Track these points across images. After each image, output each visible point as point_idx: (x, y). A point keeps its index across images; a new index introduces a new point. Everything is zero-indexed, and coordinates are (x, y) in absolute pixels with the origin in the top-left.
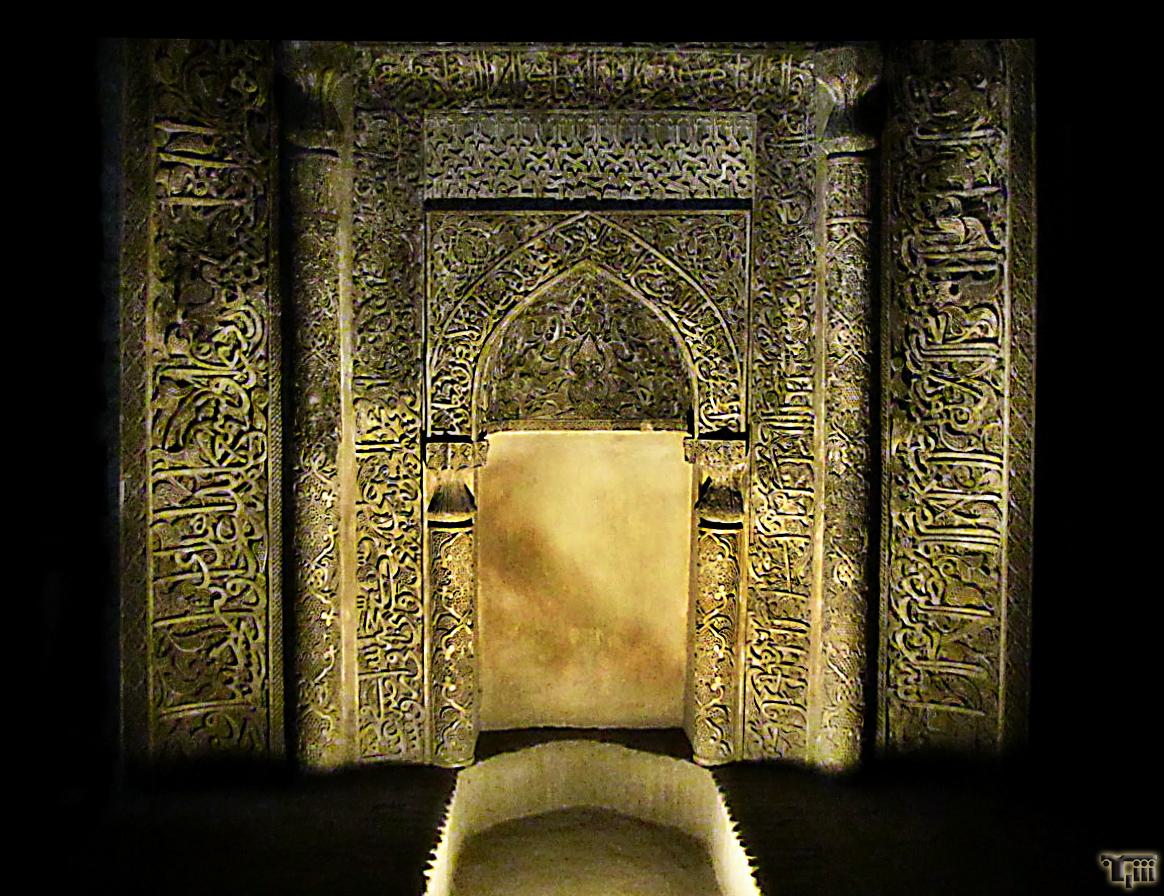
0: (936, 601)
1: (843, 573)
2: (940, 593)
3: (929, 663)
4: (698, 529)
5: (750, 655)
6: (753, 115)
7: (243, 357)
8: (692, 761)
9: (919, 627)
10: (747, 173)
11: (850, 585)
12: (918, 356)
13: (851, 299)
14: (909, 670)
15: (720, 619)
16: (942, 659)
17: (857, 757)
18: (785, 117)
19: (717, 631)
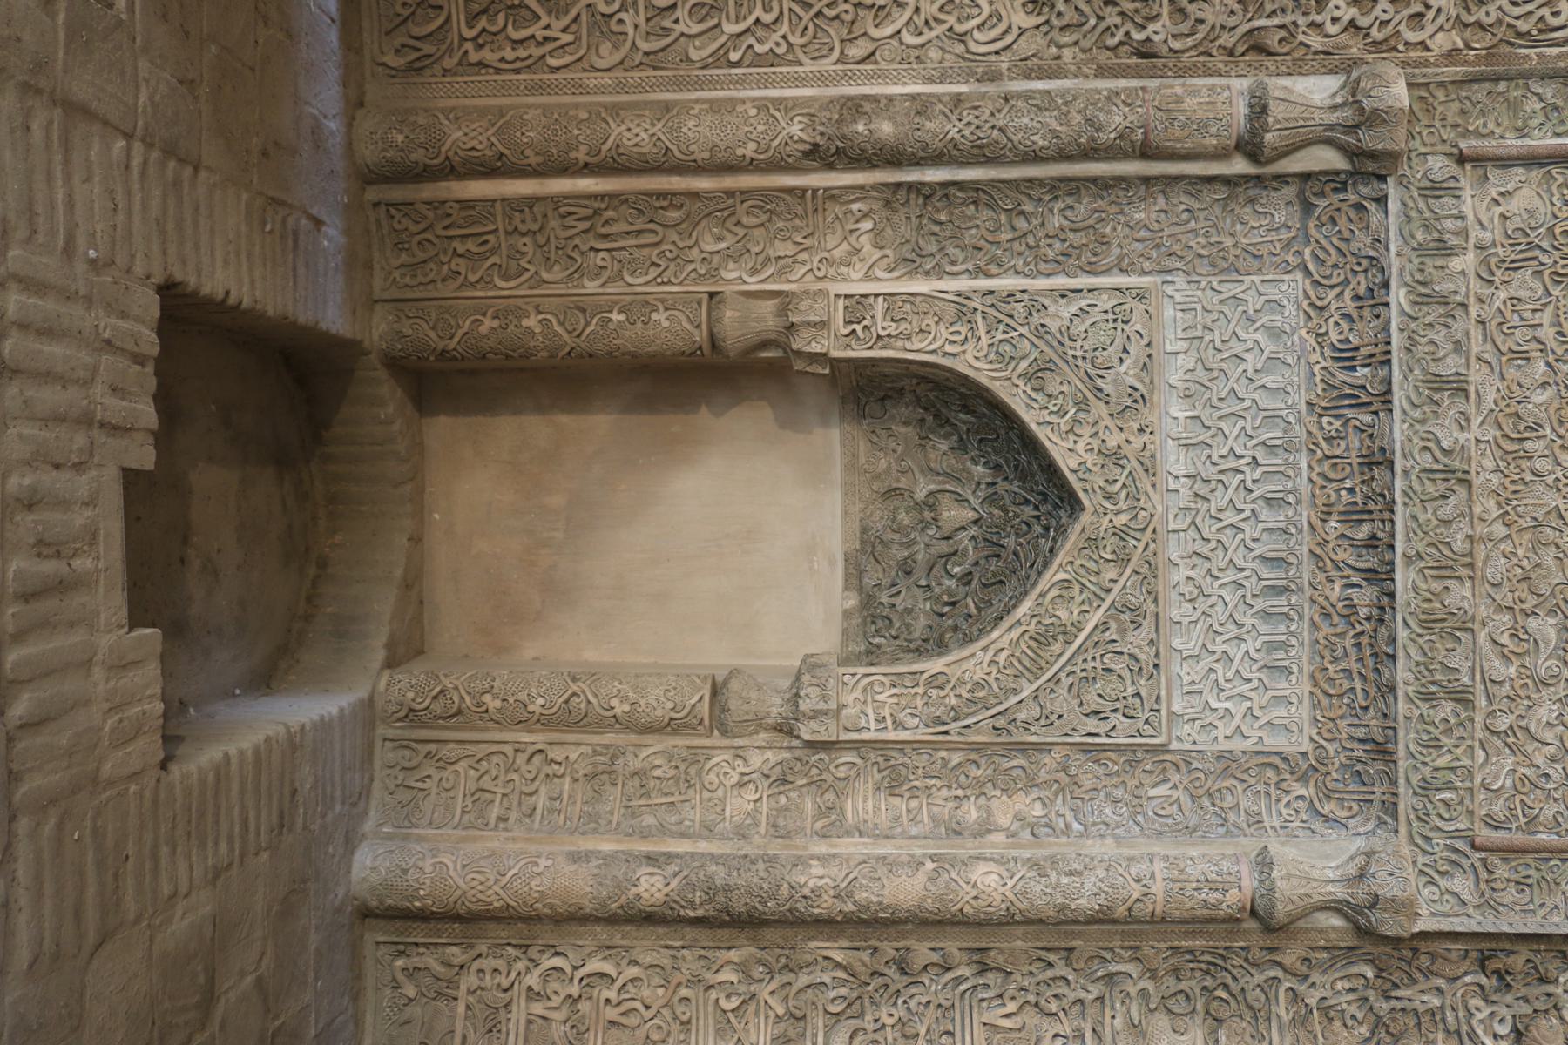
0: (611, 1013)
1: (653, 879)
2: (623, 1020)
3: (523, 1004)
4: (709, 672)
5: (531, 749)
6: (1306, 746)
7: (946, 26)
8: (382, 668)
9: (575, 990)
10: (1221, 739)
11: (634, 890)
12: (962, 988)
13: (1042, 893)
14: (513, 975)
15: (583, 706)
16: (529, 1022)
17: (390, 901)
18: (1303, 792)
19: (566, 702)
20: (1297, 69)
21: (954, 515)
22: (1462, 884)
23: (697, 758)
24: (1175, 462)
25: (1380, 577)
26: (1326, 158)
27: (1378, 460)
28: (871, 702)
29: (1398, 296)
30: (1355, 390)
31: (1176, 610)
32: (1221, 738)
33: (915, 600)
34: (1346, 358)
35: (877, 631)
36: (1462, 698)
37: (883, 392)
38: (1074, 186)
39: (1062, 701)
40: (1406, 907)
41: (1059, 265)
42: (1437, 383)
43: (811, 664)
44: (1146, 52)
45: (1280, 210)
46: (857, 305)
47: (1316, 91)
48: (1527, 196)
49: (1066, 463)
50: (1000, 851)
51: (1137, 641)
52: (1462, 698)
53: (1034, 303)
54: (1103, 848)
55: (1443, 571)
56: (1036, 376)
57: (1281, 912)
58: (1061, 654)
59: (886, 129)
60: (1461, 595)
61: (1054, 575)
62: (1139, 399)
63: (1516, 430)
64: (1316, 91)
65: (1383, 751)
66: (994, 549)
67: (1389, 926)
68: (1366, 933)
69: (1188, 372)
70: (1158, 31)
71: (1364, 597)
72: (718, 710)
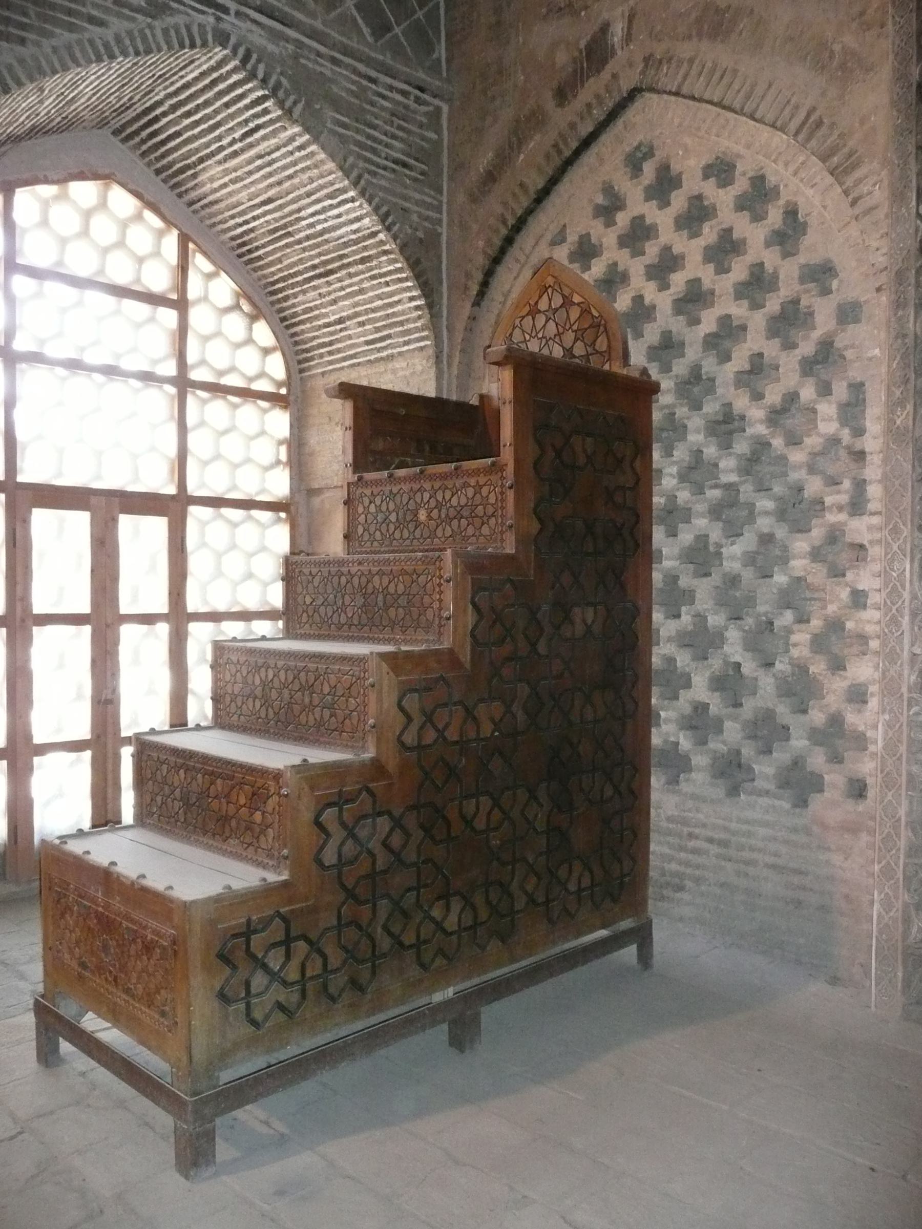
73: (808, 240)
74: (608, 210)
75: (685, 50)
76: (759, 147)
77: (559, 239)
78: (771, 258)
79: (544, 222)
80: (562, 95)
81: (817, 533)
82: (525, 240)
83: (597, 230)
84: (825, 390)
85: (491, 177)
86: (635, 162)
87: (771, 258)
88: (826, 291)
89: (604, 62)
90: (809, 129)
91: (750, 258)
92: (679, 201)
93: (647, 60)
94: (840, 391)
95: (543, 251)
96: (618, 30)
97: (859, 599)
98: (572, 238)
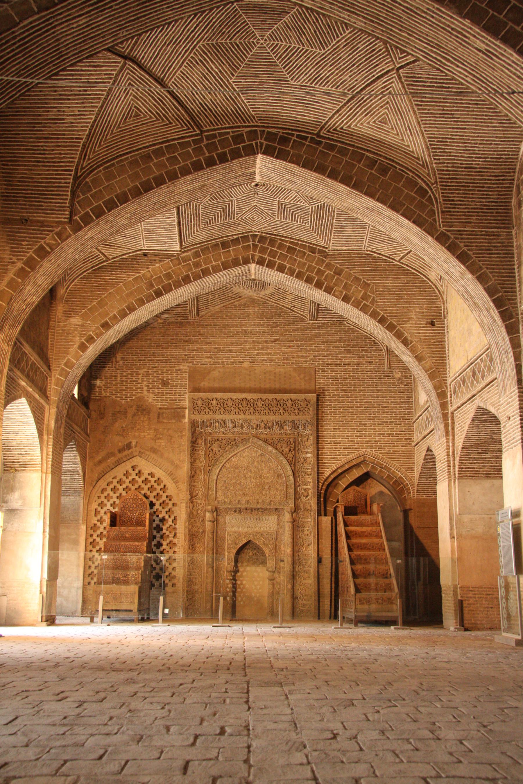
20: (205, 516)
21: (251, 554)
22: (290, 502)
23: (277, 582)
24: (246, 530)
25: (258, 509)
26: (215, 513)
27: (246, 509)
28: (271, 564)
29: (230, 506)
30: (240, 511)
31: (262, 529)
32: (275, 525)
33: (260, 559)
34: (235, 511)
35: (263, 563)
36: (271, 501)
37: (236, 561)
38: (216, 540)
39: (271, 542)
40: (291, 508)
41: (224, 542)
42: (238, 503)
43: (267, 570)
44: (203, 532)
45: (220, 518)
46: (228, 564)
47: (208, 515)
48: (220, 493)
49: (246, 541)
50: (286, 550)
51: (265, 534)
52: (271, 501)
53: (228, 544)
54: (286, 539)
55: (258, 503)
56: (236, 544)
57: (292, 520)
58: (266, 542)
59: (210, 560)
60: (260, 501)
61: (257, 543)
62: (239, 534)
63: (244, 495)
64: (208, 515)
65: (276, 509)
66: (255, 549)
67: (293, 510)
68: (295, 512)
69: (237, 528)
70: (201, 531)
71: (260, 510)
72: (272, 579)
73: (168, 491)
74: (127, 474)
75: (148, 453)
76: (159, 473)
77: (115, 478)
78: (161, 493)
79: (112, 474)
80: (120, 451)
81: (168, 541)
82: (107, 476)
83: (124, 478)
84: (169, 517)
85: (100, 462)
86: (133, 468)
87: (161, 493)
88: (170, 500)
89: (130, 449)
90: (171, 474)
91: (157, 492)
92: (143, 478)
93: (140, 452)
94: (173, 518)
95: (111, 480)
96: (133, 444)
97: (174, 552)
98: (118, 479)
